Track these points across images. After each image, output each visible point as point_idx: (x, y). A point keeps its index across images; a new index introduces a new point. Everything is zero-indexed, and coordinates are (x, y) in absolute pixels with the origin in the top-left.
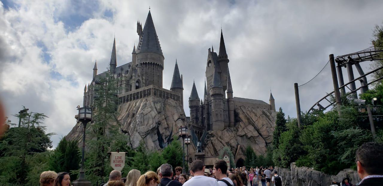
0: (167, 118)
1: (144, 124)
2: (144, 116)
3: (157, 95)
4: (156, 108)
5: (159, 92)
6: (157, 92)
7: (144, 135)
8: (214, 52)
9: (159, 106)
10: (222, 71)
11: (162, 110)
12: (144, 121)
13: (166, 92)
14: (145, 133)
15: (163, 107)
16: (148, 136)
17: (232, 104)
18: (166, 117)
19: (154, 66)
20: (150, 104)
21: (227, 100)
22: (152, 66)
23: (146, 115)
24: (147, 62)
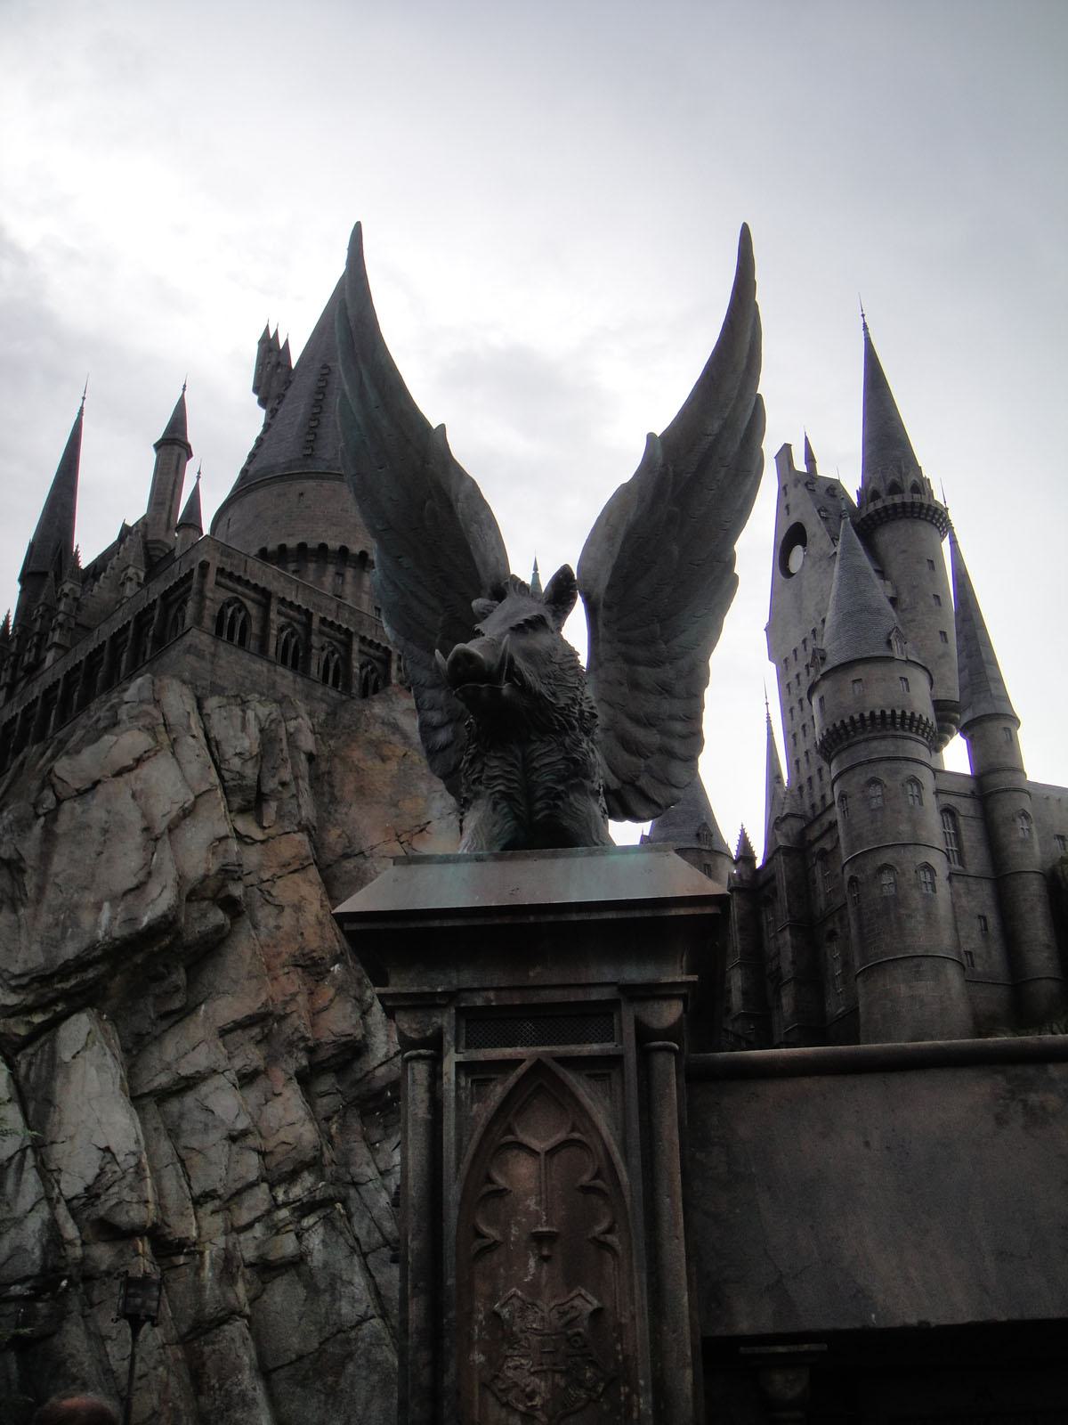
0: (349, 865)
1: (41, 889)
2: (59, 802)
3: (253, 644)
4: (212, 744)
5: (273, 616)
6: (253, 610)
7: (30, 1010)
8: (823, 470)
9: (253, 729)
10: (896, 588)
11: (286, 774)
12: (45, 858)
13: (363, 639)
14: (43, 978)
15: (311, 758)
16: (78, 1028)
17: (1025, 815)
18: (328, 857)
19: (340, 574)
20: (157, 702)
21: (971, 785)
22: (331, 569)
23: (81, 793)
24: (292, 543)
